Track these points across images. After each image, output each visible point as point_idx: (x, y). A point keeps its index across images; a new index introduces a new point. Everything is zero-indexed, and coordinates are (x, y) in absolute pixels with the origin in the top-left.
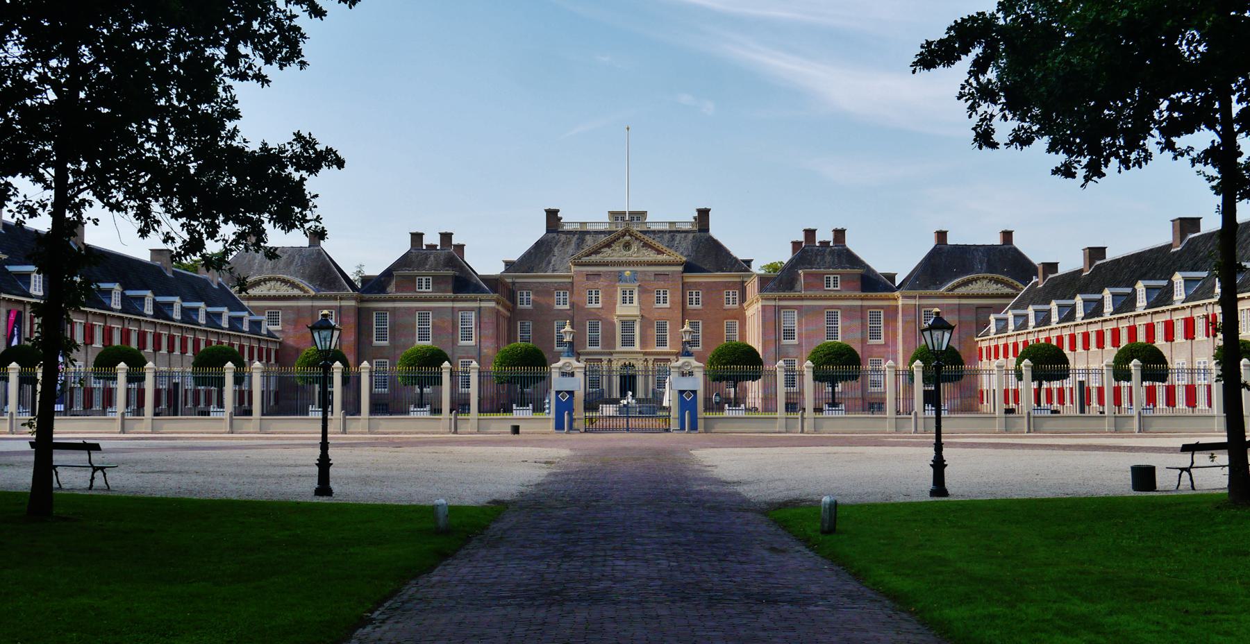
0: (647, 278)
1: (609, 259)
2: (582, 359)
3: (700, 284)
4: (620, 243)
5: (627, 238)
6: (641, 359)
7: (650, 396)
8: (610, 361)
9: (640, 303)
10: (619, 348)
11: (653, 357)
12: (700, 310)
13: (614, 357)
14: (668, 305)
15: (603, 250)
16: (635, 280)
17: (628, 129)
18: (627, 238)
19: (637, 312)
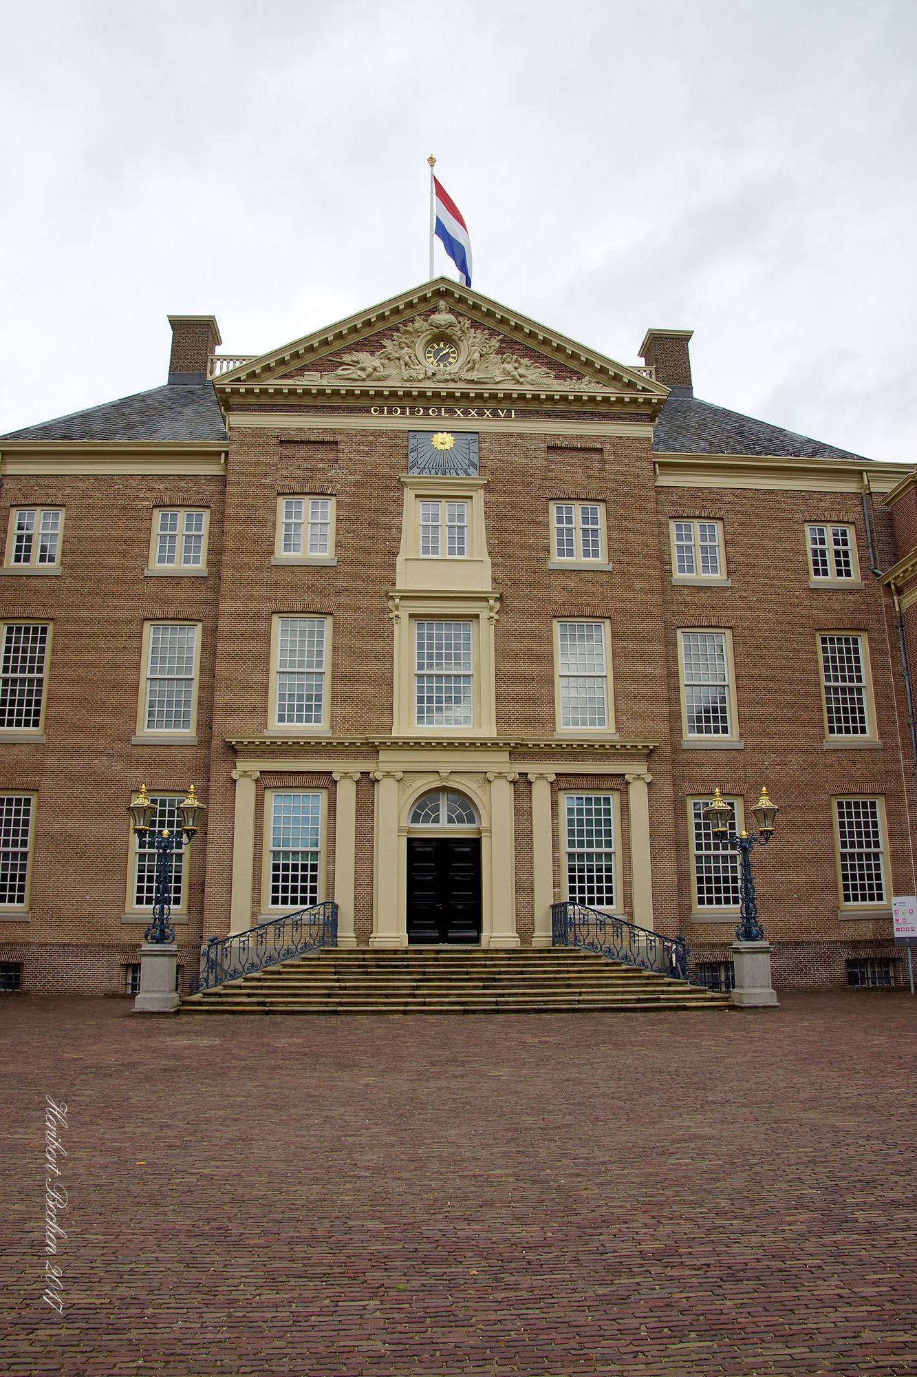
0: (521, 461)
1: (371, 386)
2: (245, 774)
3: (717, 495)
4: (417, 332)
5: (443, 318)
6: (500, 775)
7: (542, 936)
8: (367, 784)
9: (498, 551)
10: (406, 725)
11: (551, 769)
12: (722, 589)
13: (389, 762)
14: (600, 561)
15: (347, 358)
16: (472, 464)
17: (432, 160)
18: (443, 318)
19: (485, 585)
